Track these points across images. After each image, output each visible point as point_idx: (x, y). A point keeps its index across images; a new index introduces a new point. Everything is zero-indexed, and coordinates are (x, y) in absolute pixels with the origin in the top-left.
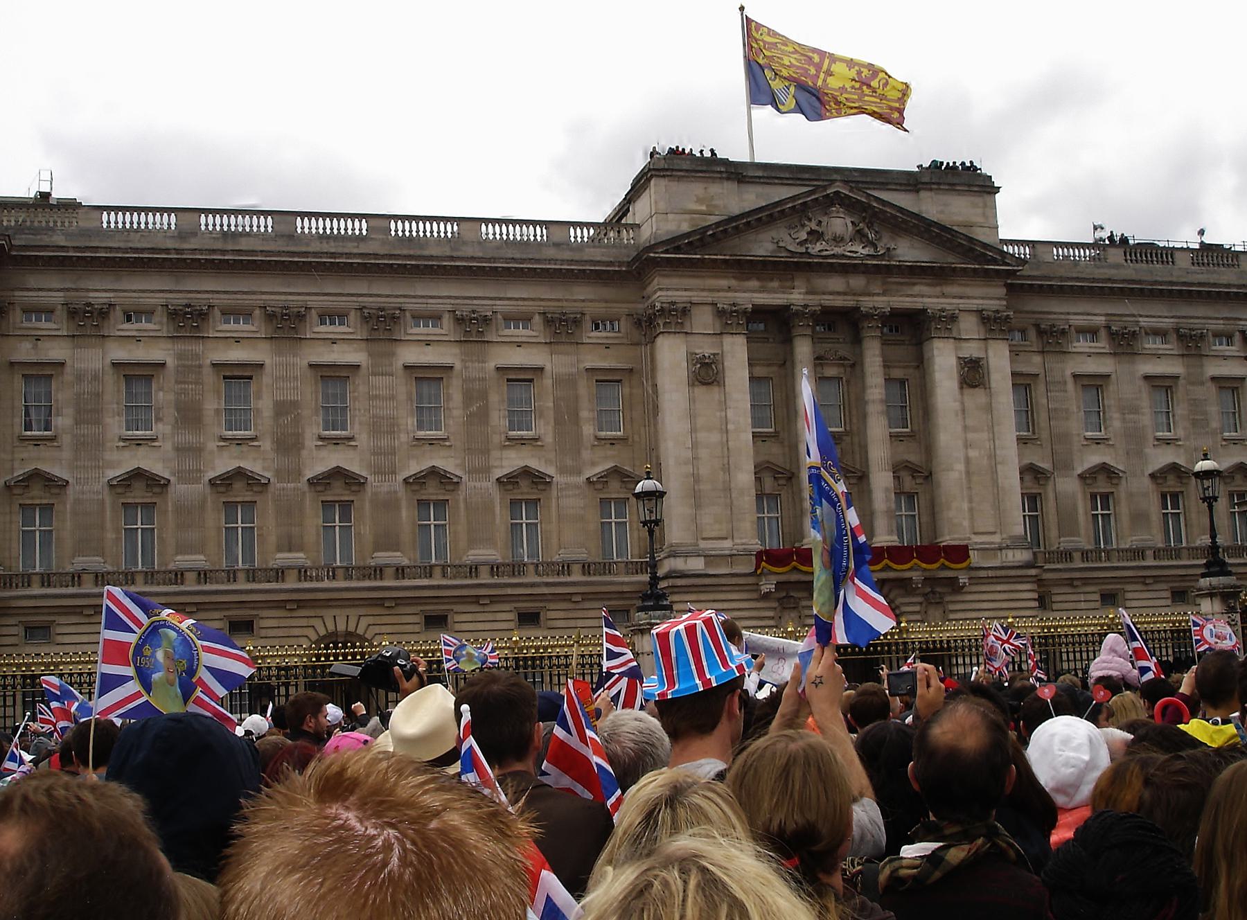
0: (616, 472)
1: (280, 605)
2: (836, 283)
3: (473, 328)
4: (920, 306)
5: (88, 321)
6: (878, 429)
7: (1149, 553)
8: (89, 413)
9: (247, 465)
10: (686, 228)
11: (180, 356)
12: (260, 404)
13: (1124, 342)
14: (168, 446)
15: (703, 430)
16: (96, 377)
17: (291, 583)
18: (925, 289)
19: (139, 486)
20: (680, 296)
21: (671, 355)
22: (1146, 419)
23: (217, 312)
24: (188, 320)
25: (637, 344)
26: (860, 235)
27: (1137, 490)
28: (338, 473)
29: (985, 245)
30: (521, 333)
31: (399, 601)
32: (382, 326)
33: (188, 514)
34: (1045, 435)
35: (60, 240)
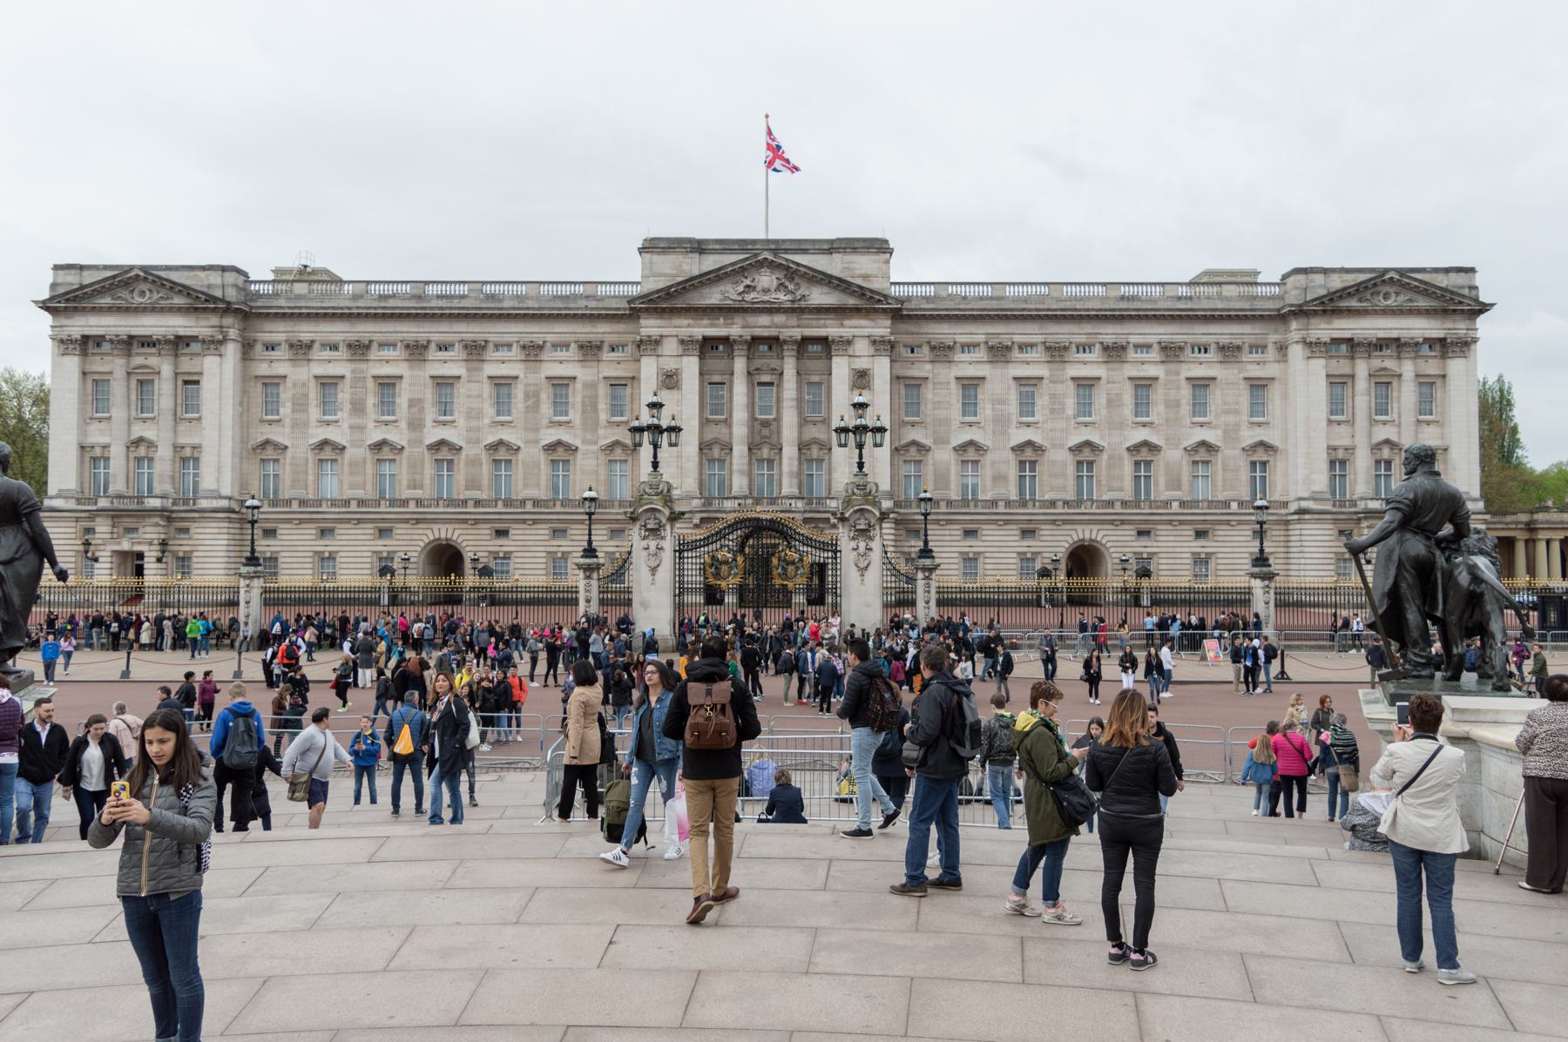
0: (617, 443)
1: (406, 521)
2: (764, 320)
3: (532, 351)
5: (301, 349)
6: (789, 419)
7: (1001, 504)
8: (300, 405)
9: (390, 437)
10: (661, 285)
11: (353, 372)
12: (398, 400)
13: (999, 353)
14: (345, 425)
16: (304, 385)
19: (328, 449)
22: (1013, 408)
23: (375, 345)
24: (359, 349)
29: (872, 291)
30: (562, 354)
31: (477, 521)
32: (475, 350)
33: (356, 466)
34: (929, 420)
35: (282, 303)
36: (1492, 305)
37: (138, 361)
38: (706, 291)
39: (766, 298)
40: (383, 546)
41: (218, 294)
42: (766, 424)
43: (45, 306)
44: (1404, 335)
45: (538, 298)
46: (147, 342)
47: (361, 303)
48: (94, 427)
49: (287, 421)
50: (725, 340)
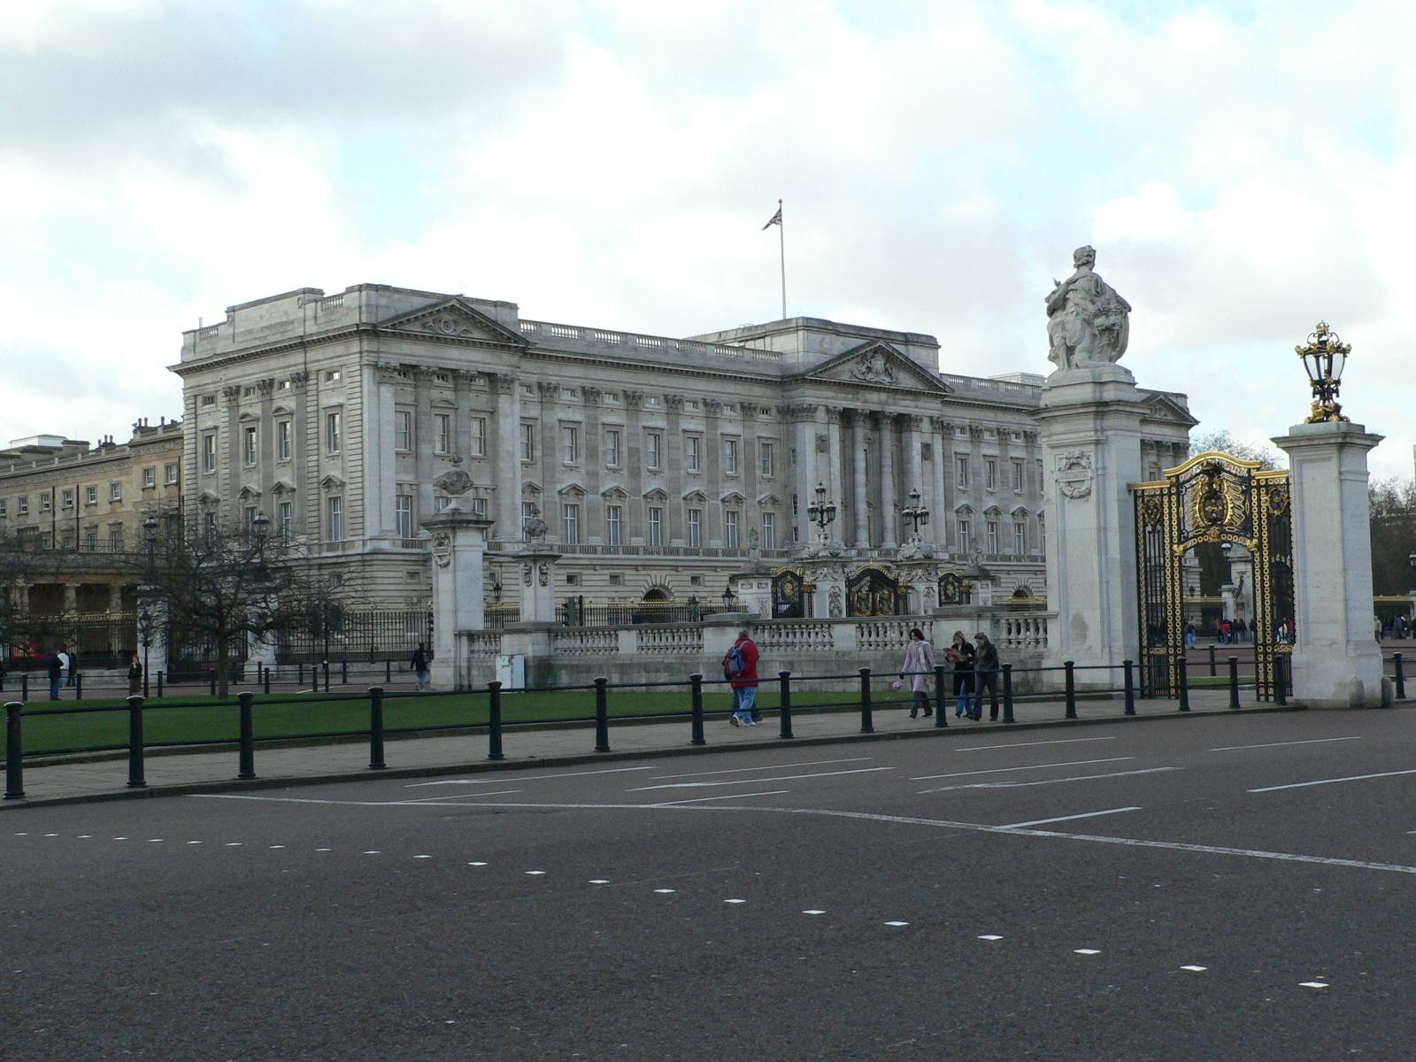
1: (636, 567)
2: (874, 396)
3: (711, 406)
4: (907, 412)
5: (547, 391)
8: (549, 450)
13: (975, 433)
14: (583, 471)
17: (641, 556)
18: (910, 403)
19: (572, 493)
21: (807, 434)
22: (983, 480)
25: (779, 423)
27: (978, 519)
32: (673, 403)
36: (1197, 422)
38: (840, 368)
39: (877, 379)
44: (1165, 439)
47: (594, 351)
49: (539, 464)
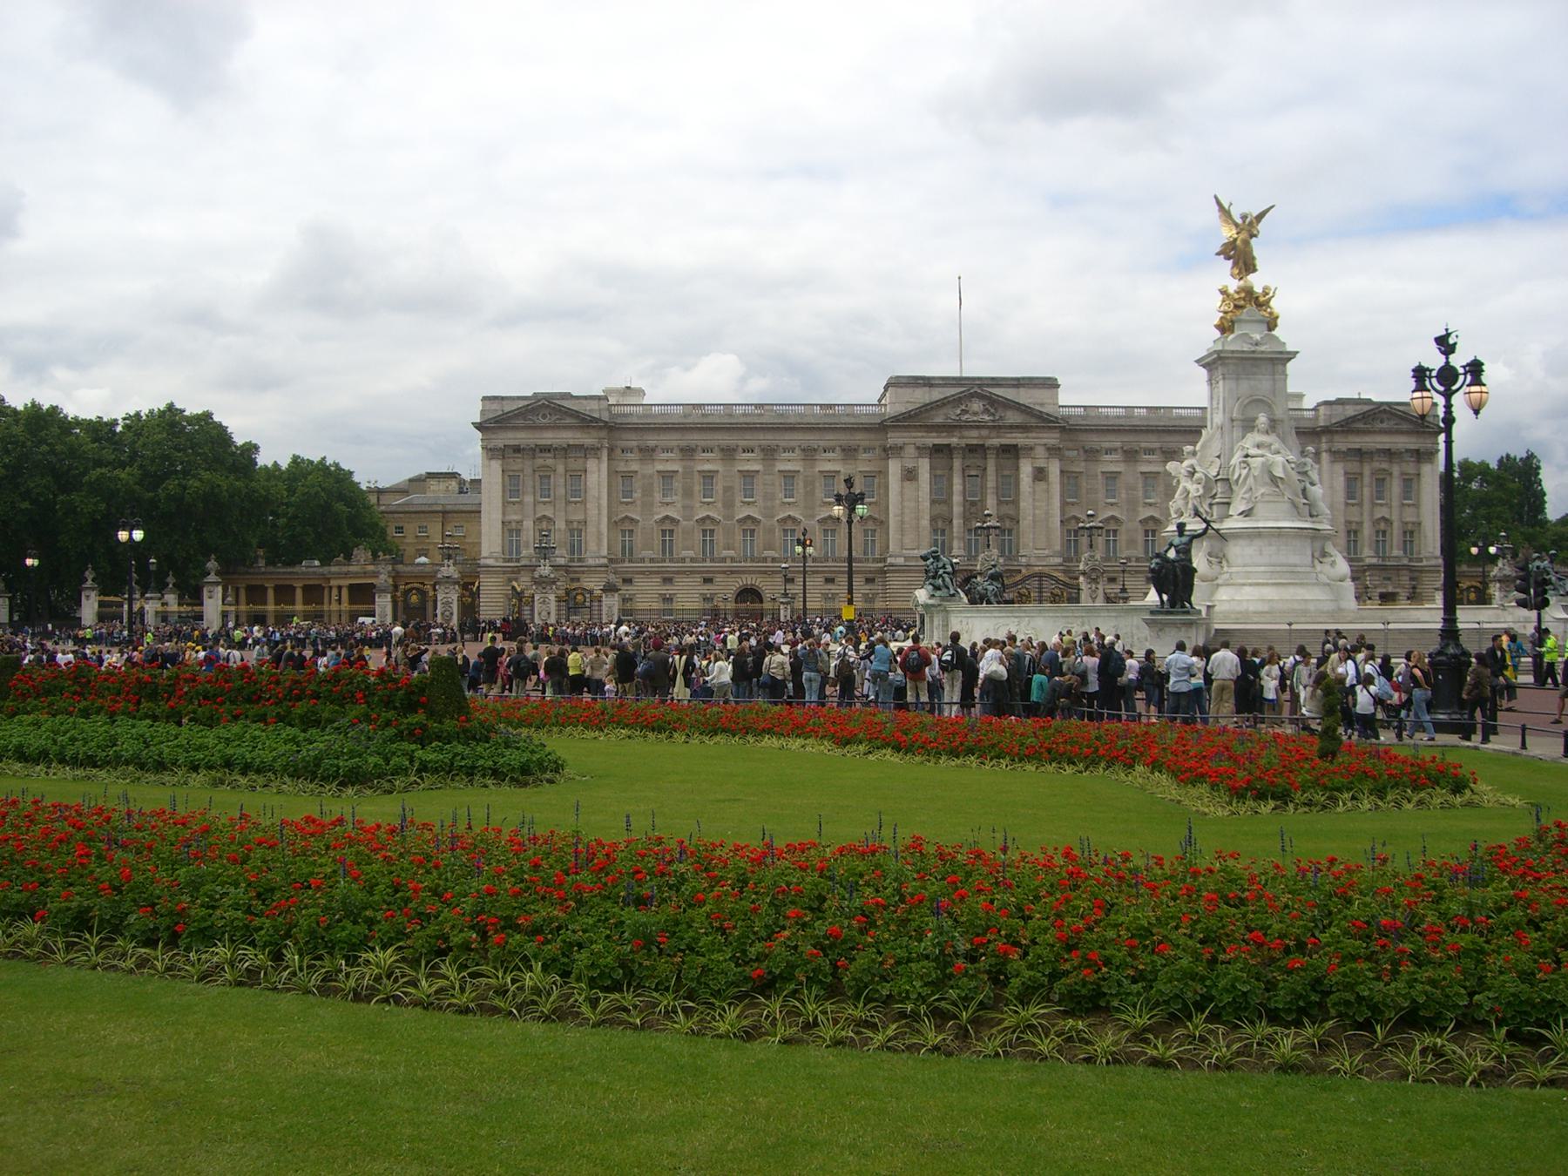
2: (974, 433)
3: (809, 453)
5: (647, 453)
8: (648, 491)
13: (1131, 455)
14: (679, 505)
15: (907, 503)
16: (651, 477)
20: (900, 441)
21: (894, 467)
22: (1140, 494)
24: (688, 452)
26: (986, 411)
28: (749, 517)
30: (830, 455)
32: (769, 453)
37: (540, 462)
40: (707, 590)
41: (596, 415)
42: (973, 504)
43: (479, 426)
45: (814, 415)
46: (546, 449)
48: (510, 508)
50: (948, 445)
